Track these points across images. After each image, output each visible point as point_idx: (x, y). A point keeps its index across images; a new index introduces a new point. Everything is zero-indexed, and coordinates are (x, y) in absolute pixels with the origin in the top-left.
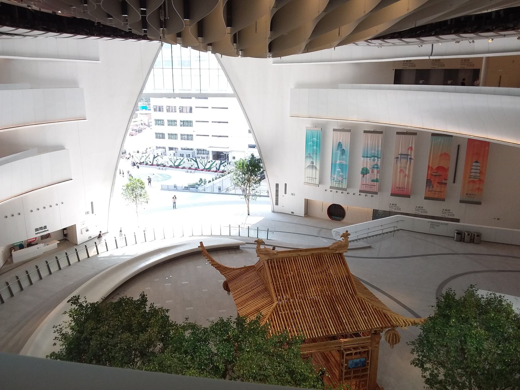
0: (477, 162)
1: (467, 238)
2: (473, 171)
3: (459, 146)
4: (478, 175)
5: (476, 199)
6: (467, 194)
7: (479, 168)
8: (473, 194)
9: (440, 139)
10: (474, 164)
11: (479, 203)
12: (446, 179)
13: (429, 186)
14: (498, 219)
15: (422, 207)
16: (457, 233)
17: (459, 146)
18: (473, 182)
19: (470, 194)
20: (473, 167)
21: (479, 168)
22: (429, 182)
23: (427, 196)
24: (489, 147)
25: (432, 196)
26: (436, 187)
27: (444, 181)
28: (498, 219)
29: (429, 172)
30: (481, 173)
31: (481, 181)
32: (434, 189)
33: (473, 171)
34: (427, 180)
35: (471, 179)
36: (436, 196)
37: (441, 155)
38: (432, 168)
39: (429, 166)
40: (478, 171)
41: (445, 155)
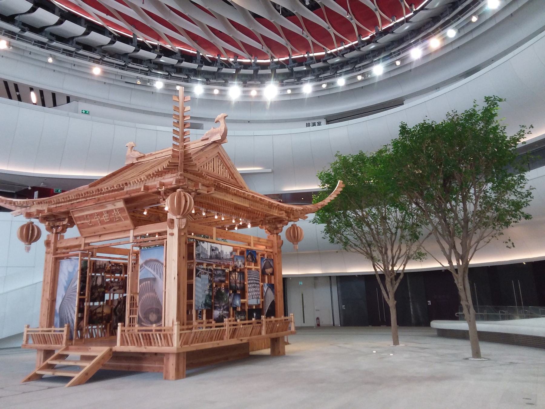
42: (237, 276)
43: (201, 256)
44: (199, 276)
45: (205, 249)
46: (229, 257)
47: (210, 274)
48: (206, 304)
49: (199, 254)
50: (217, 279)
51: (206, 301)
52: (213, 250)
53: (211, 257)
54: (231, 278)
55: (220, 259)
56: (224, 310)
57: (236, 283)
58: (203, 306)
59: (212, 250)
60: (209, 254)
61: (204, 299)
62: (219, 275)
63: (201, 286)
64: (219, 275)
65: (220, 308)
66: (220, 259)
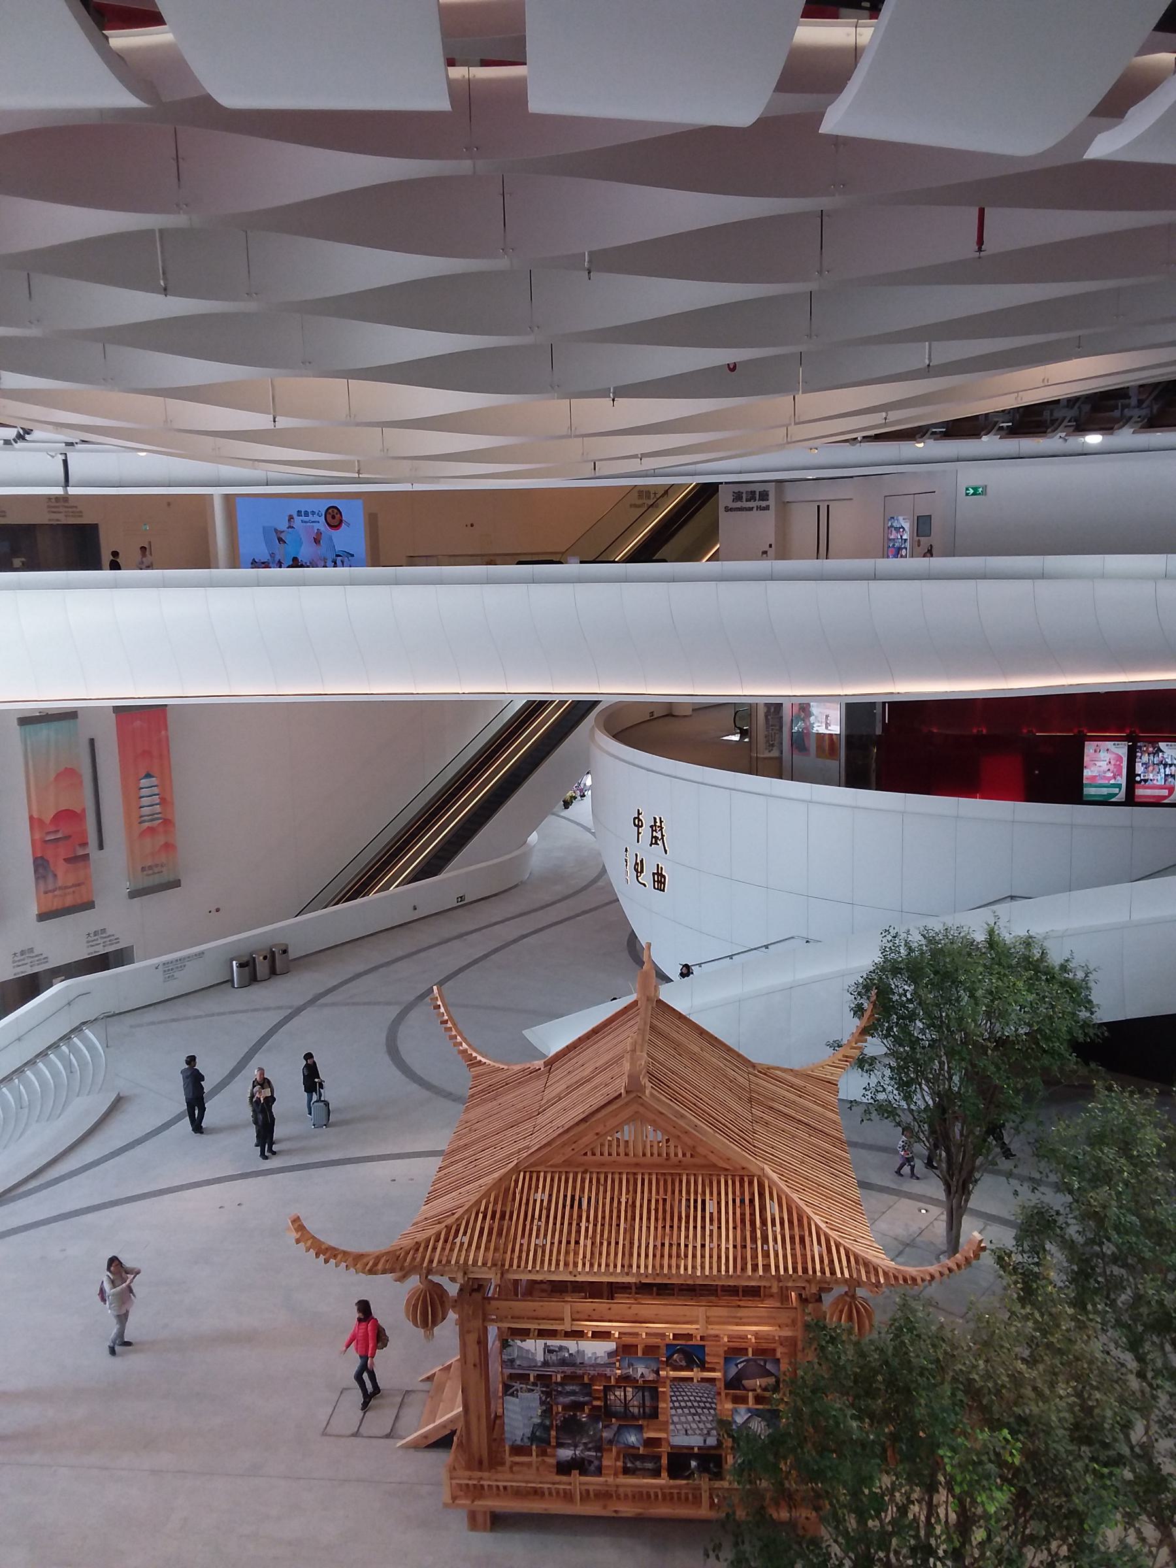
0: (148, 776)
1: (262, 968)
2: (145, 801)
3: (92, 741)
4: (158, 808)
5: (166, 877)
6: (143, 869)
7: (156, 790)
8: (157, 866)
9: (45, 732)
10: (144, 782)
11: (176, 884)
12: (84, 844)
13: (44, 877)
14: (218, 910)
15: (31, 950)
16: (241, 966)
17: (92, 741)
18: (151, 830)
19: (150, 867)
20: (144, 792)
21: (156, 790)
22: (41, 865)
23: (44, 910)
24: (166, 729)
25: (57, 904)
26: (64, 874)
27: (81, 852)
28: (218, 910)
29: (37, 836)
30: (163, 801)
31: (167, 822)
32: (60, 883)
33: (145, 801)
34: (35, 860)
35: (147, 824)
36: (69, 901)
37: (58, 776)
38: (40, 821)
39: (31, 818)
40: (156, 799)
41: (69, 774)
42: (630, 1395)
43: (518, 1362)
44: (512, 1395)
45: (528, 1351)
46: (606, 1360)
47: (542, 1392)
48: (533, 1438)
49: (512, 1361)
50: (568, 1400)
51: (533, 1433)
52: (551, 1351)
53: (545, 1363)
54: (612, 1397)
55: (574, 1365)
56: (589, 1450)
57: (626, 1405)
58: (526, 1440)
59: (548, 1350)
60: (540, 1358)
61: (528, 1432)
62: (573, 1393)
63: (518, 1409)
64: (573, 1393)
65: (576, 1446)
66: (574, 1365)
